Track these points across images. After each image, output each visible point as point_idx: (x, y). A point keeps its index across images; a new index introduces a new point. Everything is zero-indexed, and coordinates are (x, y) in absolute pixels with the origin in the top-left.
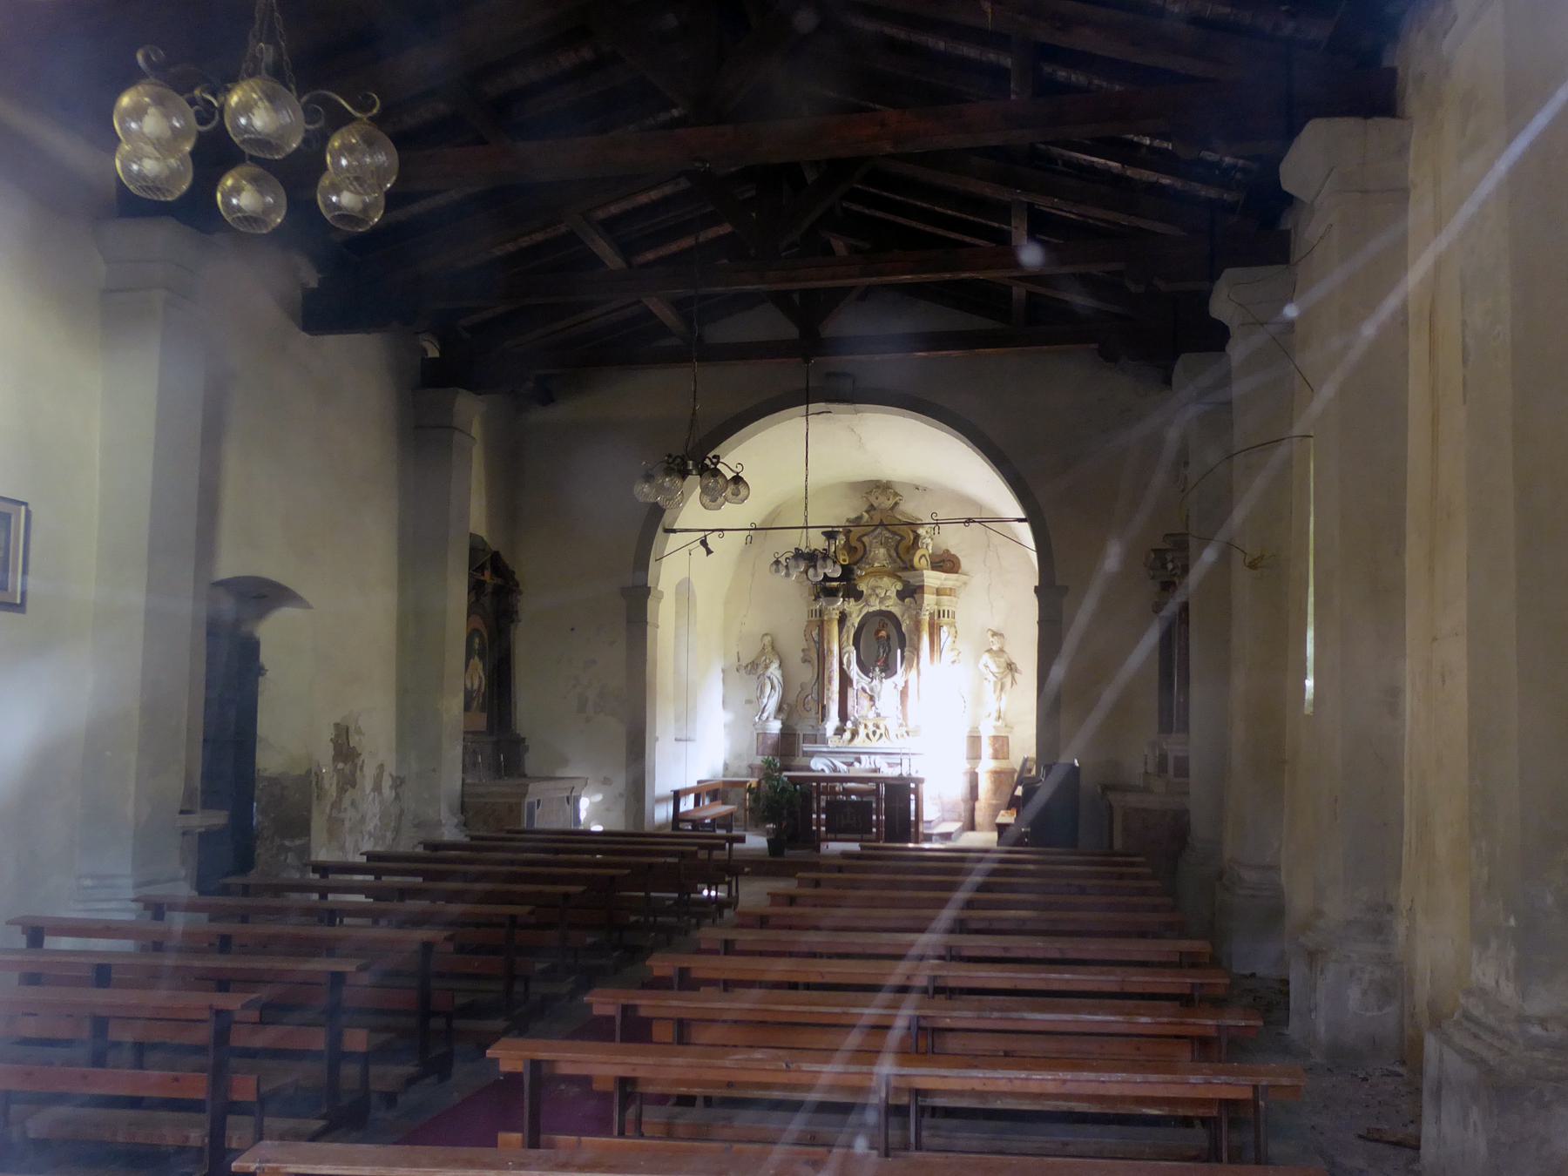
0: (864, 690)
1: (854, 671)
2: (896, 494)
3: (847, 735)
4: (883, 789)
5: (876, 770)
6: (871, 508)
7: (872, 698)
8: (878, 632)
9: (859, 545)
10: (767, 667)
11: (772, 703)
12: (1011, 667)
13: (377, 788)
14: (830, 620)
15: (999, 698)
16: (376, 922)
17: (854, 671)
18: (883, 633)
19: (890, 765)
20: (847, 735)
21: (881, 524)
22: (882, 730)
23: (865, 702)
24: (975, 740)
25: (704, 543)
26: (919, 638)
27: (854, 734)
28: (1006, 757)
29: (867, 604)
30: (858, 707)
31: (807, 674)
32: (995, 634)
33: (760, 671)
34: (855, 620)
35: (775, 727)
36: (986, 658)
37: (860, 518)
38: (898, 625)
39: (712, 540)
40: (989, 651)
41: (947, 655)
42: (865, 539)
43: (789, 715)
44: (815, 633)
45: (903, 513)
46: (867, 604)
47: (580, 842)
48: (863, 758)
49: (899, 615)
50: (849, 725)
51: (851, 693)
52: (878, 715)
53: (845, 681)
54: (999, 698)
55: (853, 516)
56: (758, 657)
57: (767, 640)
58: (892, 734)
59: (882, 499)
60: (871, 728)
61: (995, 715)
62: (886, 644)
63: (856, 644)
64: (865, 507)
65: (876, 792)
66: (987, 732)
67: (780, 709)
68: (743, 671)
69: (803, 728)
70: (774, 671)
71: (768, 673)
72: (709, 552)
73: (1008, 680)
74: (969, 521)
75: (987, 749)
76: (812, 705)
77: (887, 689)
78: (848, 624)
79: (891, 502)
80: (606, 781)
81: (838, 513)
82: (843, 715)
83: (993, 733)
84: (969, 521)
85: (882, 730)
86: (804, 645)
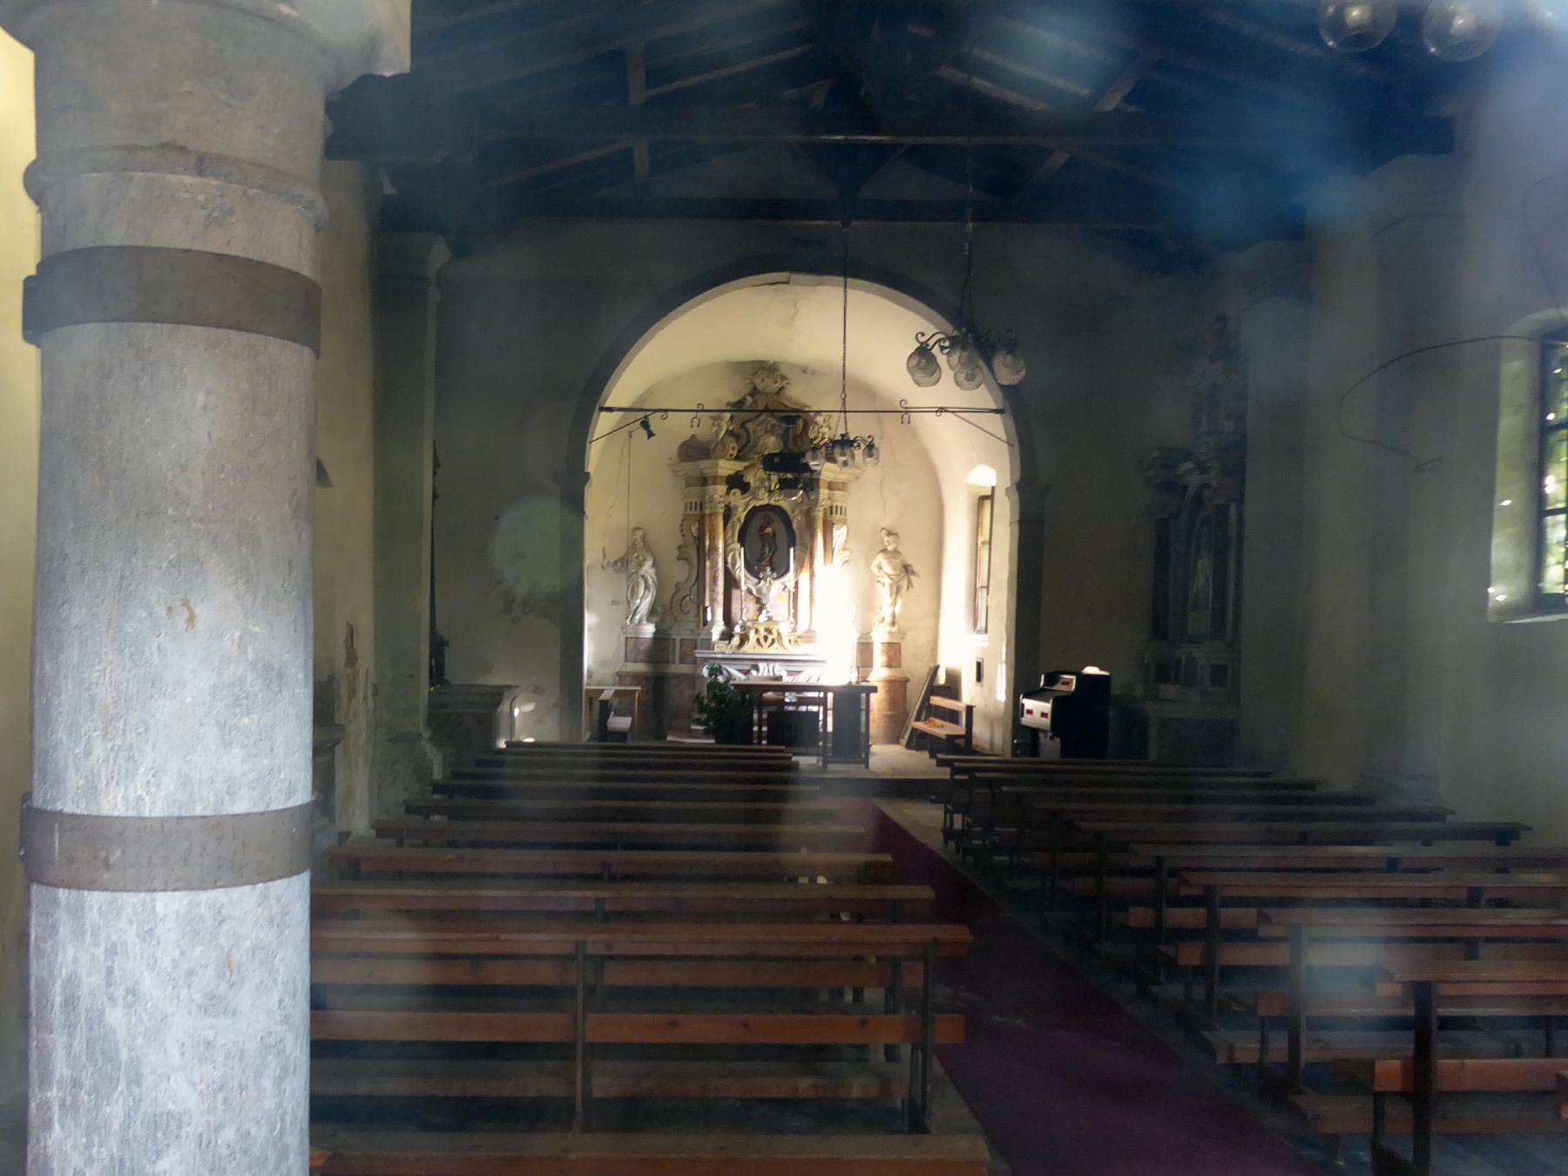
0: (749, 591)
1: (741, 572)
2: (784, 378)
3: (736, 640)
4: (830, 696)
5: (780, 678)
6: (754, 392)
7: (758, 600)
8: (762, 528)
9: (742, 432)
10: (640, 565)
11: (644, 603)
12: (907, 569)
13: (365, 698)
14: (713, 515)
15: (895, 603)
16: (400, 844)
17: (741, 572)
18: (769, 530)
19: (790, 673)
20: (736, 640)
21: (766, 410)
22: (775, 636)
23: (753, 606)
24: (865, 648)
25: (645, 424)
26: (813, 537)
27: (744, 639)
28: (899, 666)
29: (755, 497)
30: (744, 610)
31: (680, 573)
32: (889, 534)
33: (632, 569)
34: (741, 514)
35: (649, 630)
36: (880, 559)
37: (741, 402)
38: (787, 522)
39: (654, 420)
40: (884, 551)
41: (839, 556)
42: (750, 426)
43: (663, 619)
44: (694, 529)
45: (789, 399)
46: (755, 497)
47: (624, 756)
48: (761, 665)
49: (789, 510)
50: (737, 629)
51: (735, 593)
52: (770, 619)
53: (731, 582)
54: (895, 603)
55: (734, 399)
56: (627, 554)
57: (639, 534)
58: (785, 642)
59: (768, 381)
60: (762, 633)
61: (889, 619)
62: (775, 542)
63: (742, 540)
64: (747, 390)
65: (822, 702)
66: (880, 636)
67: (652, 612)
68: (610, 570)
69: (679, 633)
70: (648, 569)
71: (642, 572)
72: (651, 435)
73: (904, 583)
74: (942, 410)
75: (879, 658)
76: (691, 607)
77: (776, 591)
78: (734, 519)
79: (778, 385)
80: (538, 690)
81: (724, 393)
82: (728, 619)
83: (886, 639)
84: (942, 410)
85: (775, 636)
86: (679, 541)
